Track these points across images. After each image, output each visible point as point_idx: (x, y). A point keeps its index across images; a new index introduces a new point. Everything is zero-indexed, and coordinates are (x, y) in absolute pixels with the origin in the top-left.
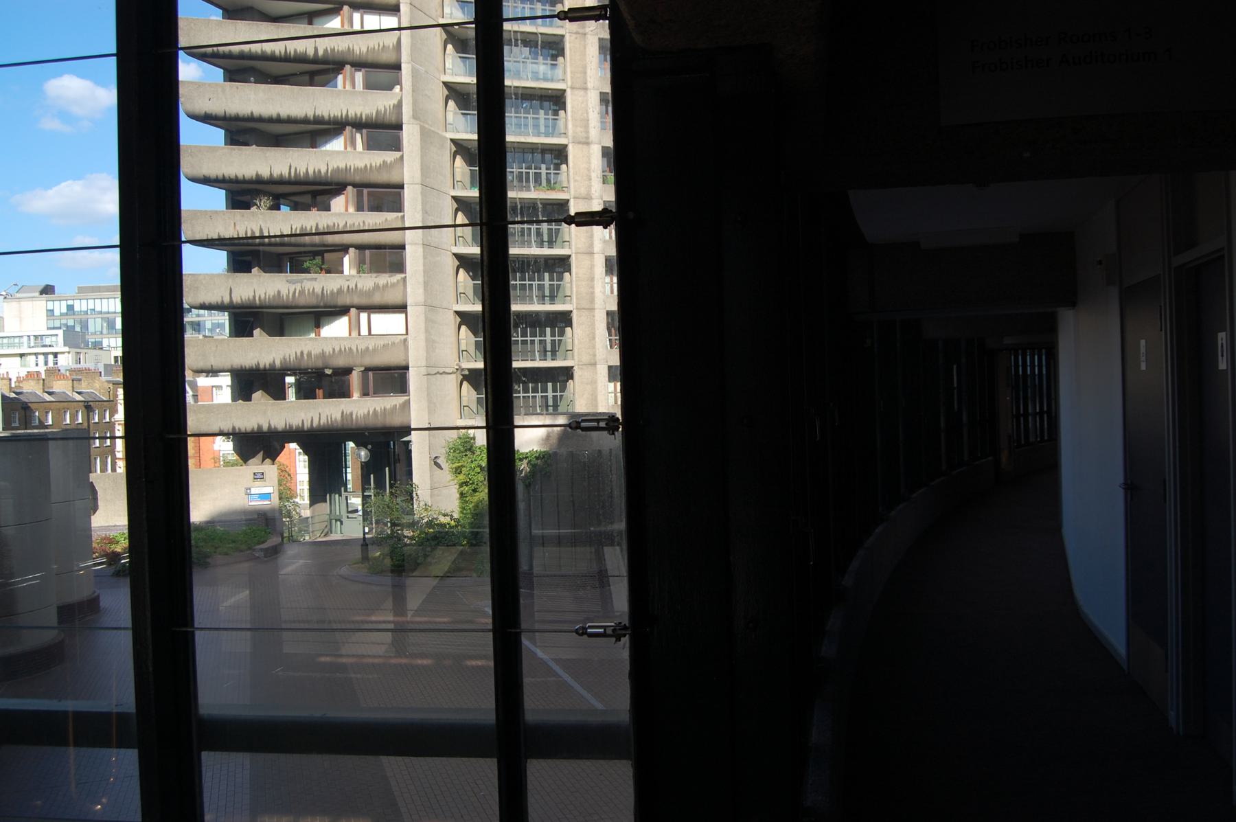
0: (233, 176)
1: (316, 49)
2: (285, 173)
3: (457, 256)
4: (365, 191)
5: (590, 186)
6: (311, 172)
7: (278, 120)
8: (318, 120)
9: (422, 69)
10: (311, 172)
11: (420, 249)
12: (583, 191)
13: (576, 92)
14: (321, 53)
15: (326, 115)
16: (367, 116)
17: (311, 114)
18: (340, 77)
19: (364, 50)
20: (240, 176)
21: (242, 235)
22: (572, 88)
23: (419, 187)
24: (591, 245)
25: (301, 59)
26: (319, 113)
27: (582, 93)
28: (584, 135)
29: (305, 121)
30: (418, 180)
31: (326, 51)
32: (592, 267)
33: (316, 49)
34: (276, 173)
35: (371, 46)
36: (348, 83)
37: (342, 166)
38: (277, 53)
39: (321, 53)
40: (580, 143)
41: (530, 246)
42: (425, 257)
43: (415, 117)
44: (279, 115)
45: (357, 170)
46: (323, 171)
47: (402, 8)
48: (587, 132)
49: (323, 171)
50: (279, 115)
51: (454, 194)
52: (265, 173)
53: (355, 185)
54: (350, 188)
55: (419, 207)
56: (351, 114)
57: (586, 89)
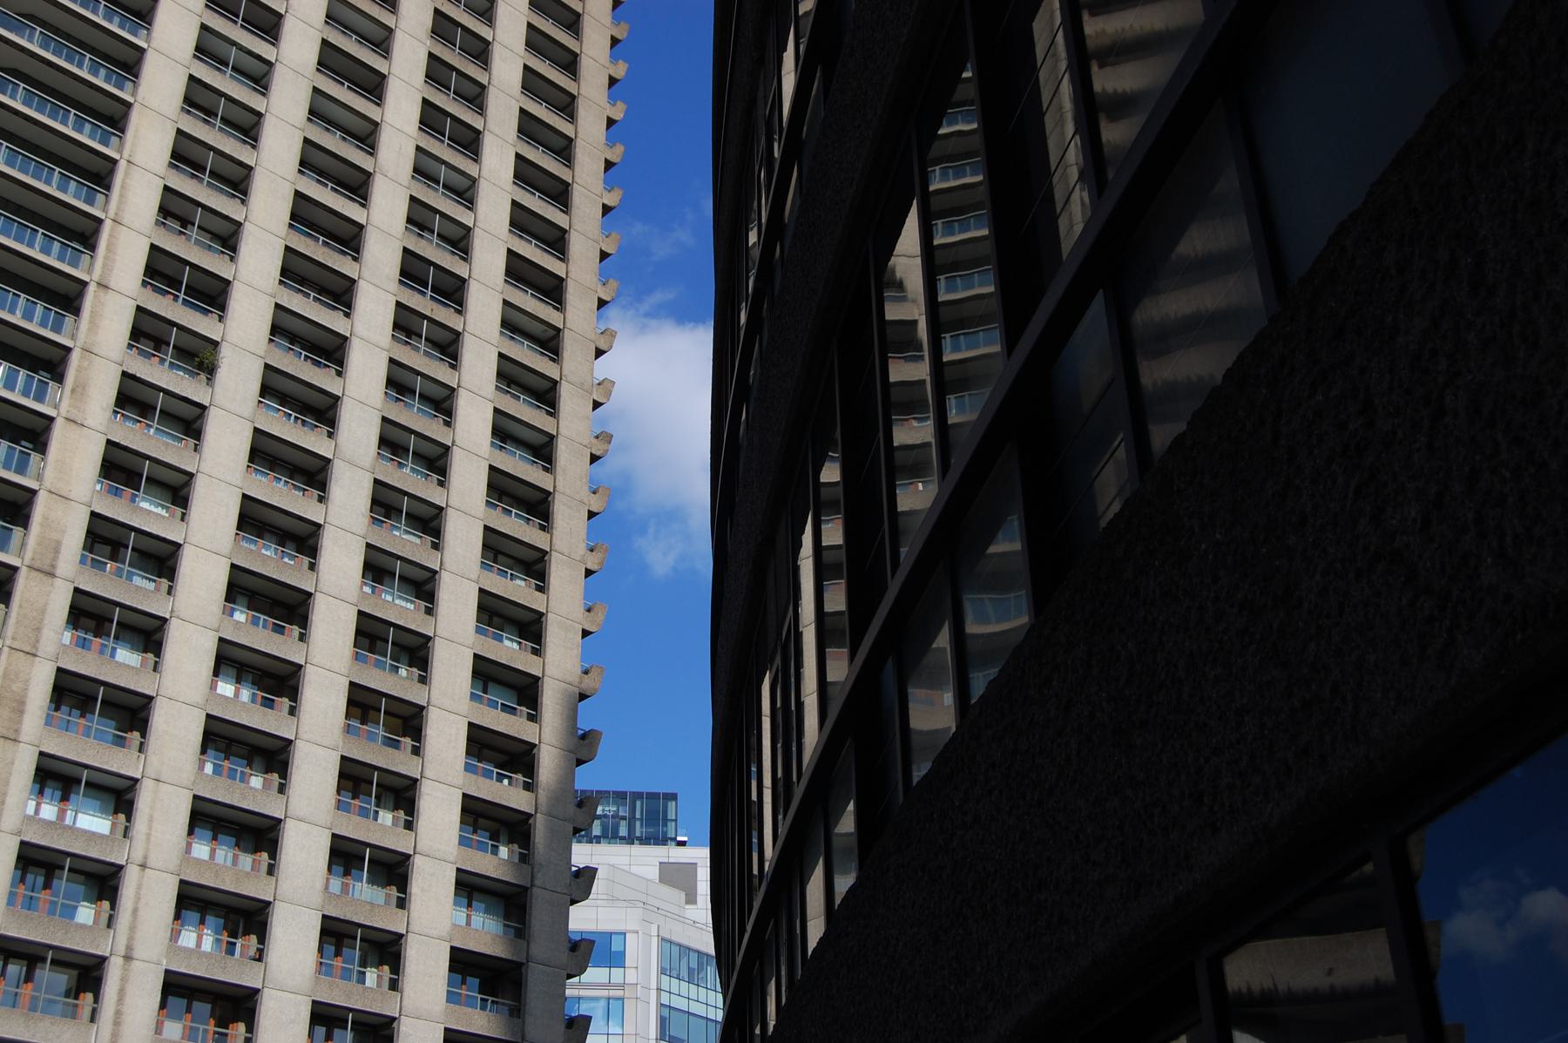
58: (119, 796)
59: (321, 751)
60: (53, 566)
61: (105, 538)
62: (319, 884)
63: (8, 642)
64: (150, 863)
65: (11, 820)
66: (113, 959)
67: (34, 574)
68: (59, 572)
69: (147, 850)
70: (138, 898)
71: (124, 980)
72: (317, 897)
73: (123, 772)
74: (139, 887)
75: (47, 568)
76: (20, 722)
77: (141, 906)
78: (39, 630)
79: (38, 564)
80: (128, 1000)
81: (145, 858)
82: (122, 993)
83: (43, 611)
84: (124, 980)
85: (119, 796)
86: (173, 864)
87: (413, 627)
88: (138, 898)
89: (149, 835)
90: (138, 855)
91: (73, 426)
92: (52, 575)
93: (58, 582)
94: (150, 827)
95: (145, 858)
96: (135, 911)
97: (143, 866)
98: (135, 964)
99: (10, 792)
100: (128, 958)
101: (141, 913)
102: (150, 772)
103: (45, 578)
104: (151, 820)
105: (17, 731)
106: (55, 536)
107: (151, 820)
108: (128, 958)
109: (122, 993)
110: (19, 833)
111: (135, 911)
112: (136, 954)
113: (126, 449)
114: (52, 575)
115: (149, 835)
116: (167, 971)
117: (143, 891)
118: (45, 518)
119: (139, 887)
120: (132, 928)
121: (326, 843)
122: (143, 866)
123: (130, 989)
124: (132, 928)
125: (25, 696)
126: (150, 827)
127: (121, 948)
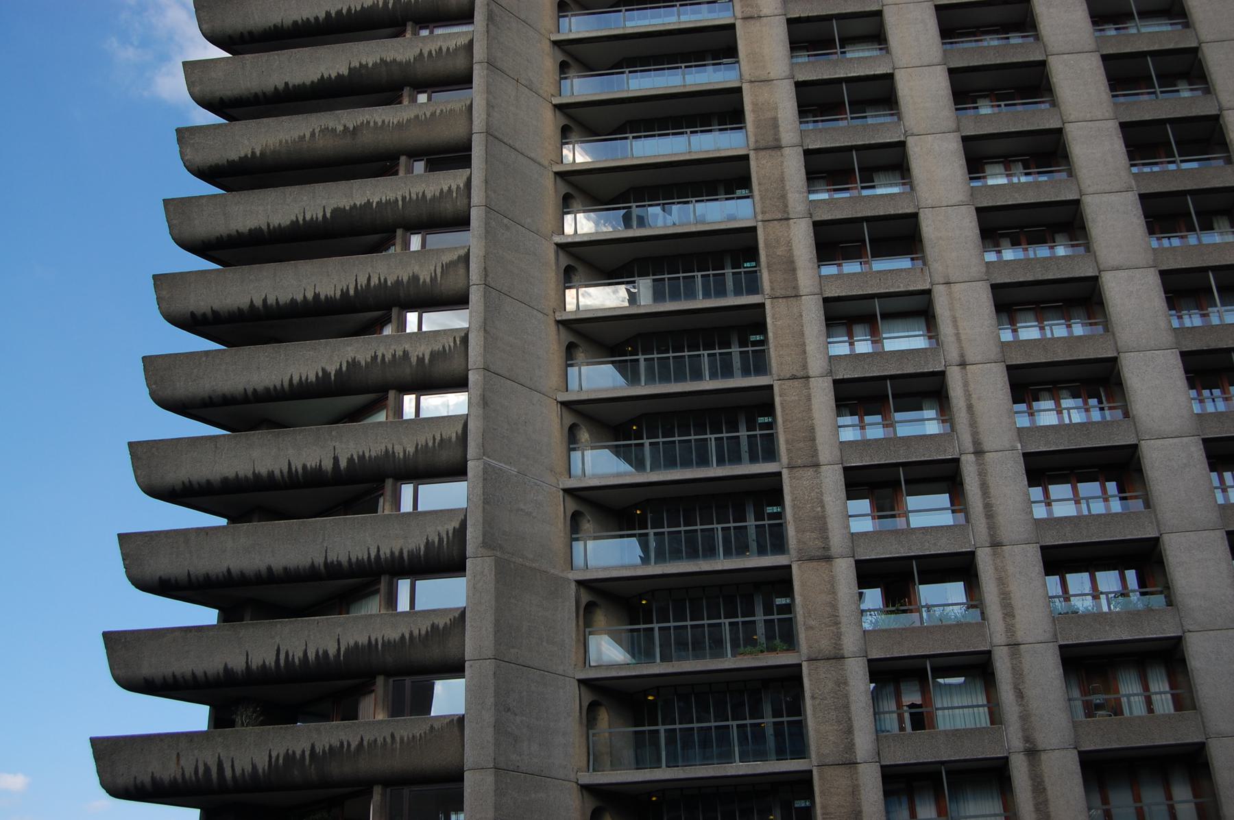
0: (188, 675)
1: (336, 460)
2: (270, 660)
3: (587, 789)
4: (408, 681)
5: (838, 636)
6: (311, 656)
7: (269, 579)
8: (333, 571)
9: (514, 471)
10: (311, 656)
11: (490, 778)
12: (825, 645)
13: (799, 473)
14: (343, 464)
15: (344, 559)
16: (411, 553)
17: (319, 561)
18: (381, 500)
19: (411, 449)
20: (199, 672)
21: (189, 772)
22: (791, 467)
23: (489, 666)
24: (850, 747)
25: (313, 480)
26: (332, 557)
27: (810, 472)
28: (819, 544)
29: (310, 575)
30: (490, 654)
31: (351, 460)
32: (855, 791)
33: (336, 460)
34: (256, 662)
35: (422, 441)
36: (387, 506)
37: (362, 640)
38: (277, 473)
39: (343, 464)
40: (811, 559)
41: (727, 757)
42: (499, 792)
43: (488, 543)
44: (270, 569)
45: (388, 645)
46: (332, 652)
47: (472, 377)
48: (826, 539)
49: (332, 652)
50: (270, 569)
51: (583, 676)
52: (237, 663)
53: (388, 673)
54: (380, 680)
55: (490, 700)
56: (385, 552)
57: (817, 465)
58: (918, 309)
59: (1113, 198)
60: (778, 140)
61: (815, 101)
62: (1163, 324)
63: (760, 217)
64: (970, 358)
65: (816, 365)
66: (963, 458)
67: (762, 153)
68: (784, 142)
69: (961, 348)
70: (968, 396)
71: (982, 474)
72: (1168, 338)
73: (911, 288)
74: (966, 385)
75: (772, 144)
76: (796, 279)
77: (974, 402)
78: (783, 197)
79: (762, 144)
80: (993, 491)
81: (962, 356)
82: (985, 488)
83: (782, 180)
84: (982, 474)
85: (918, 309)
86: (994, 352)
87: (1171, 46)
88: (968, 396)
89: (957, 335)
90: (953, 354)
91: (752, 22)
92: (779, 147)
93: (787, 151)
94: (956, 326)
95: (962, 356)
96: (970, 408)
97: (963, 364)
98: (989, 457)
99: (807, 342)
100: (979, 452)
101: (979, 407)
102: (938, 278)
103: (773, 153)
104: (955, 321)
105: (796, 288)
106: (769, 115)
107: (955, 321)
108: (979, 452)
109: (985, 488)
110: (830, 373)
111: (970, 408)
112: (986, 447)
113: (808, 19)
114: (779, 147)
115: (957, 335)
116: (1026, 455)
117: (972, 387)
118: (754, 104)
119: (966, 385)
120: (973, 424)
121: (1152, 281)
122: (963, 364)
123: (992, 481)
124: (973, 424)
125: (792, 256)
126: (956, 326)
127: (968, 445)
